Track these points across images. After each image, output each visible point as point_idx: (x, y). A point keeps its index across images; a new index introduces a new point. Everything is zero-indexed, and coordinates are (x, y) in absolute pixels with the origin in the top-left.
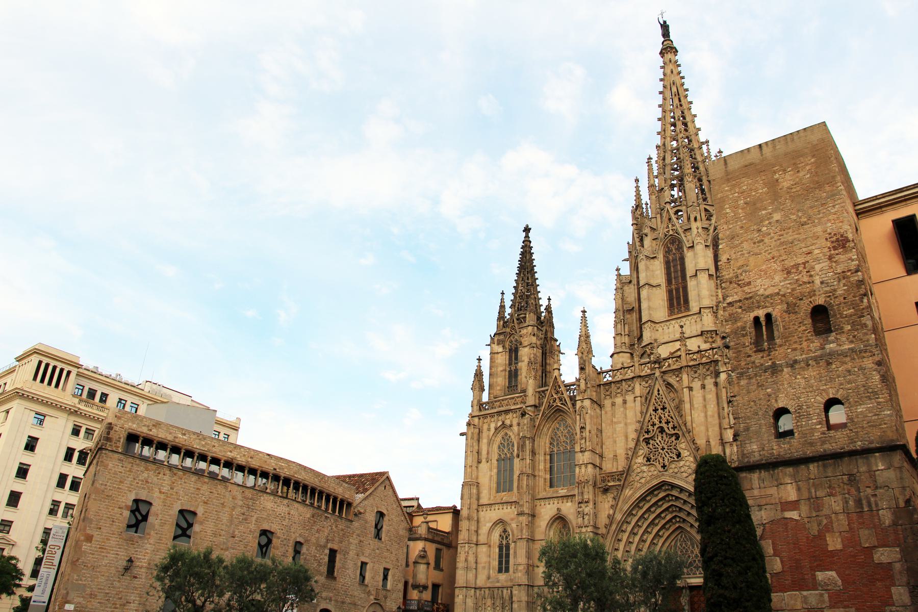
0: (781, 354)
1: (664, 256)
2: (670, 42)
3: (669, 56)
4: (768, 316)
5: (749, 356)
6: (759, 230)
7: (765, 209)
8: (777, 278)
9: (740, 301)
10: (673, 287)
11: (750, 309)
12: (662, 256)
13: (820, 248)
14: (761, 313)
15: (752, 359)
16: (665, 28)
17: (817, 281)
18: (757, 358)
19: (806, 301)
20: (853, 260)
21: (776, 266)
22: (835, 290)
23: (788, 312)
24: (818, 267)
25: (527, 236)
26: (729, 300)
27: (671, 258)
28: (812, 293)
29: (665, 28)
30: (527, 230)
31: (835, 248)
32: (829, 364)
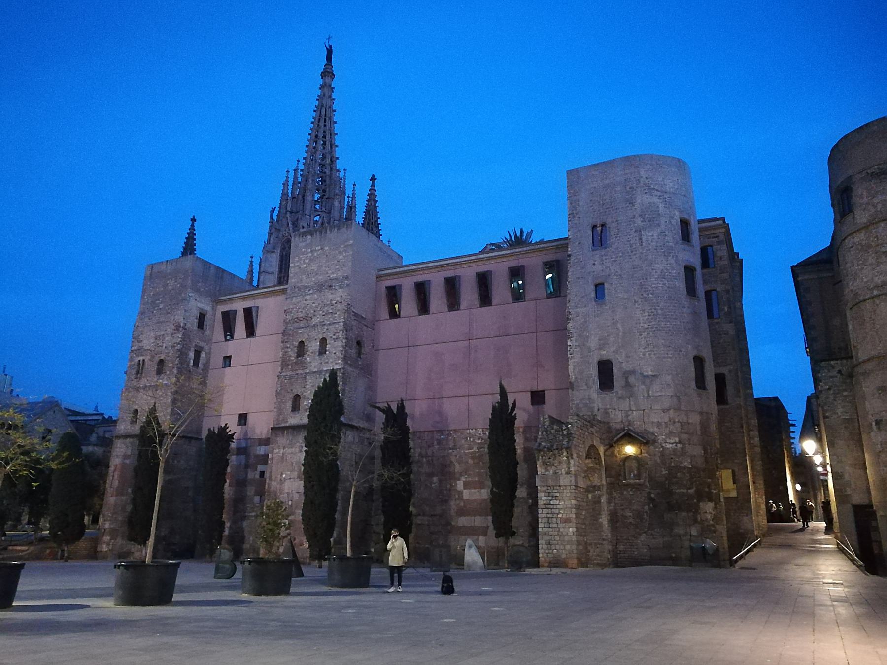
0: (144, 382)
1: (281, 251)
2: (330, 66)
3: (328, 80)
4: (144, 360)
5: (132, 380)
6: (153, 312)
7: (159, 300)
8: (152, 341)
9: (136, 350)
10: (283, 275)
11: (138, 356)
12: (279, 251)
13: (170, 328)
14: (141, 358)
15: (133, 382)
16: (330, 52)
17: (164, 347)
18: (134, 383)
19: (158, 356)
20: (179, 338)
21: (152, 334)
22: (169, 353)
23: (150, 360)
24: (166, 339)
25: (193, 225)
26: (133, 348)
27: (284, 253)
28: (161, 353)
29: (330, 52)
30: (193, 220)
31: (175, 330)
32: (156, 390)
